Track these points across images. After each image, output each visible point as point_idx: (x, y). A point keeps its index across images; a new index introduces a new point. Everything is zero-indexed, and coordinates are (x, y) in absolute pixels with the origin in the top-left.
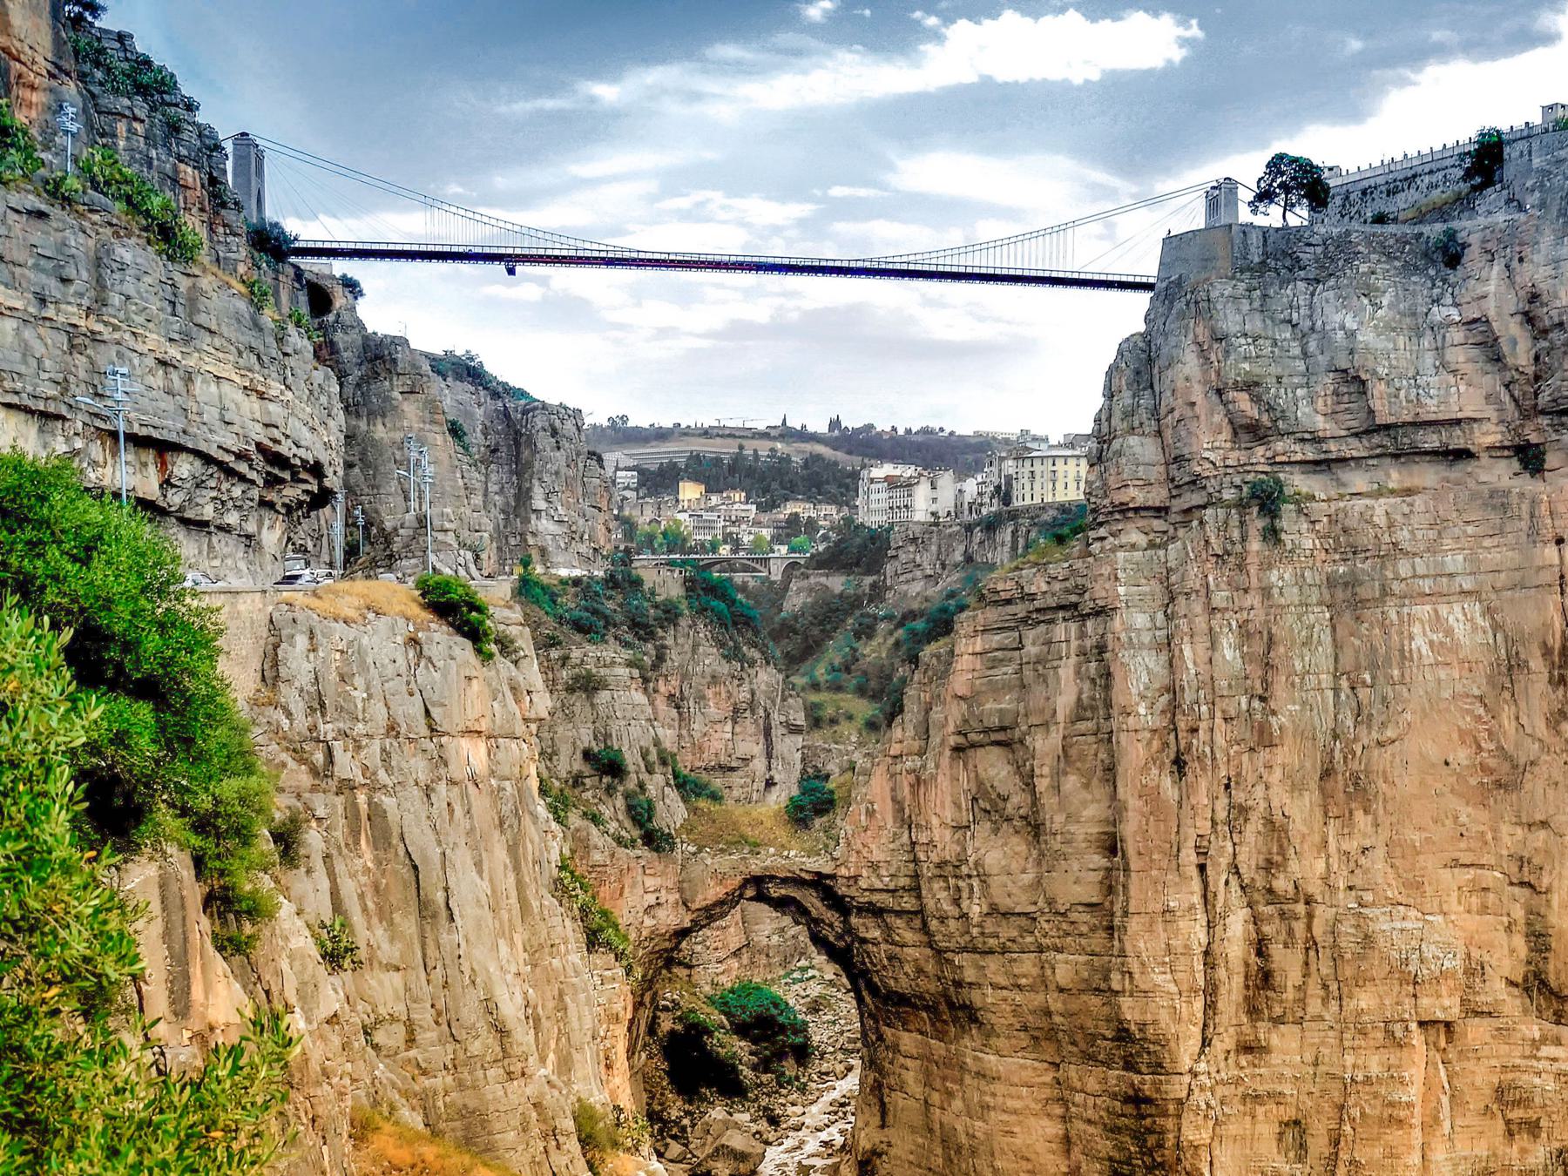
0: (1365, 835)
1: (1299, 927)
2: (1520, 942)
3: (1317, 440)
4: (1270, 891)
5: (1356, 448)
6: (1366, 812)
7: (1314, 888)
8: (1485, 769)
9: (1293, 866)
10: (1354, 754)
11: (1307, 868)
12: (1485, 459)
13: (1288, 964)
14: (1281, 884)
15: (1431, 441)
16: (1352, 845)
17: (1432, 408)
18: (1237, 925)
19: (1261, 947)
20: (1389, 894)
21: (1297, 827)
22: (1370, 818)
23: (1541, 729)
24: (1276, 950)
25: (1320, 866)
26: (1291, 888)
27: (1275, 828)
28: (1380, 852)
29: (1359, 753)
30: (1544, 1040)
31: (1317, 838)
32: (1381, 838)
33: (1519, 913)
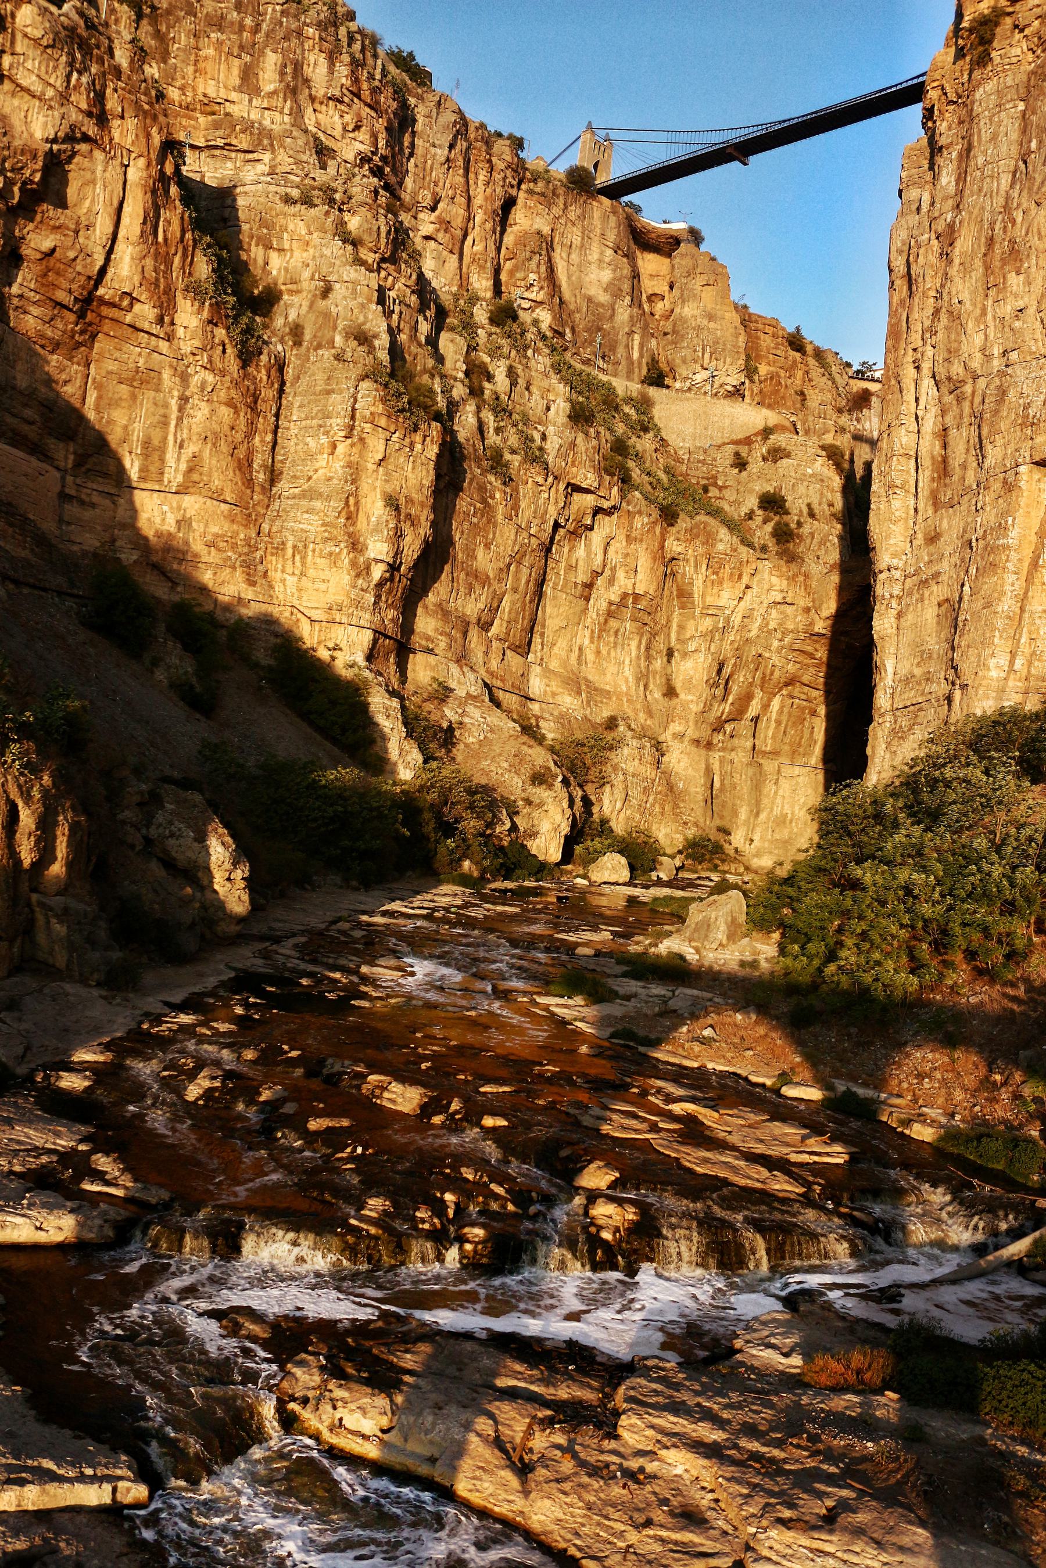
0: (1016, 295)
1: (966, 405)
4: (949, 379)
6: (1018, 273)
7: (976, 364)
9: (964, 347)
10: (1013, 222)
14: (957, 370)
16: (1007, 309)
20: (1034, 348)
22: (1021, 277)
24: (953, 432)
25: (978, 339)
26: (961, 370)
27: (955, 317)
28: (1032, 310)
29: (1019, 219)
31: (978, 312)
32: (1034, 297)
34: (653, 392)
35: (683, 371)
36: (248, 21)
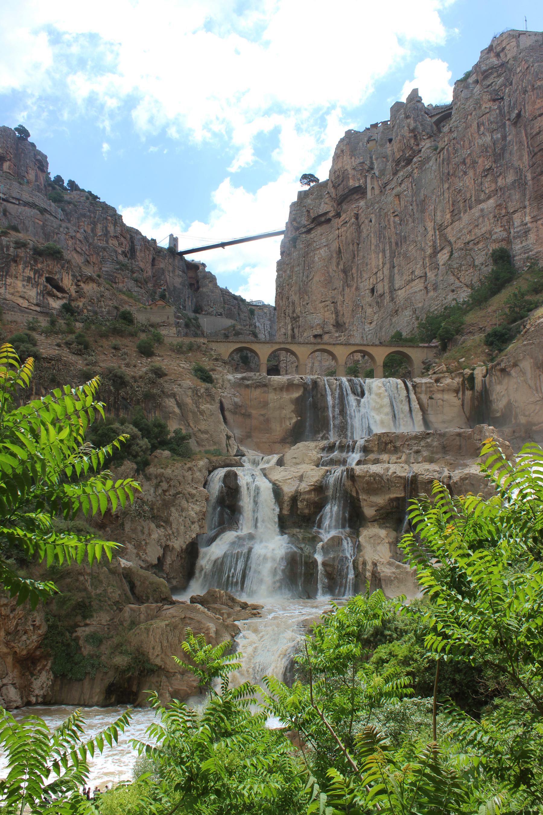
2: (334, 315)
3: (305, 226)
5: (312, 226)
8: (326, 280)
11: (298, 310)
12: (333, 219)
13: (296, 331)
14: (295, 315)
15: (323, 219)
16: (304, 303)
17: (321, 212)
18: (290, 327)
19: (293, 329)
21: (296, 302)
23: (335, 268)
30: (339, 337)
33: (333, 309)
34: (198, 315)
35: (206, 308)
36: (92, 215)
